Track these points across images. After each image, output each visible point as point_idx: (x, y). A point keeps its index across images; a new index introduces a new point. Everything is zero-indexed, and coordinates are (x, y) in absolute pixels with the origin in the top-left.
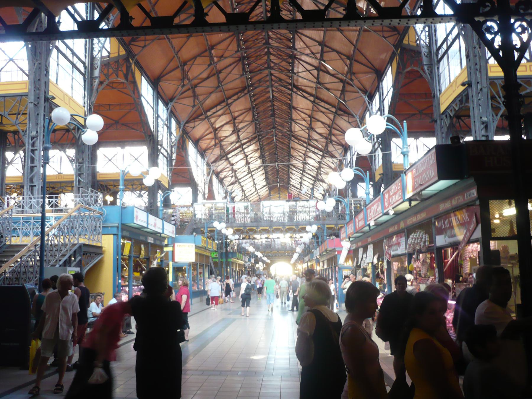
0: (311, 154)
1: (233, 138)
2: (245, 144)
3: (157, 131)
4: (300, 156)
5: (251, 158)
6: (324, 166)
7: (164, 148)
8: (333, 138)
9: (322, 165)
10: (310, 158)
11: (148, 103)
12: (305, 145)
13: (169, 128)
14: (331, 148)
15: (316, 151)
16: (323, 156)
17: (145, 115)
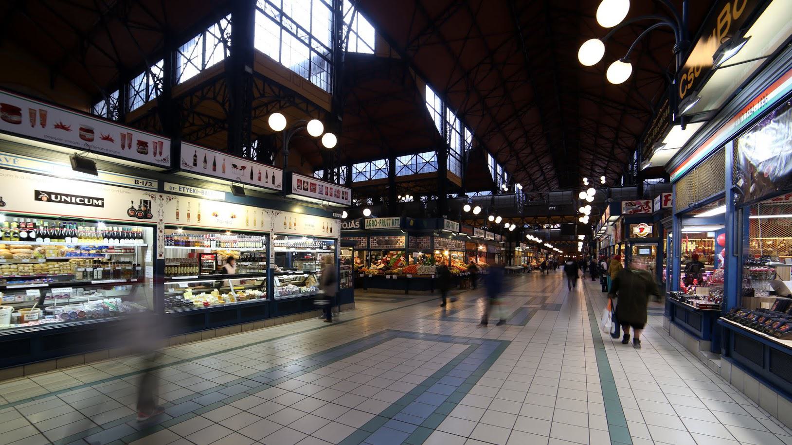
0: (598, 162)
1: (528, 150)
2: (539, 157)
3: (446, 136)
4: (587, 165)
5: (547, 169)
6: (610, 172)
7: (456, 153)
8: (620, 142)
9: (608, 171)
10: (597, 165)
11: (435, 111)
12: (592, 153)
13: (462, 136)
14: (617, 151)
15: (602, 157)
16: (609, 161)
17: (433, 123)
